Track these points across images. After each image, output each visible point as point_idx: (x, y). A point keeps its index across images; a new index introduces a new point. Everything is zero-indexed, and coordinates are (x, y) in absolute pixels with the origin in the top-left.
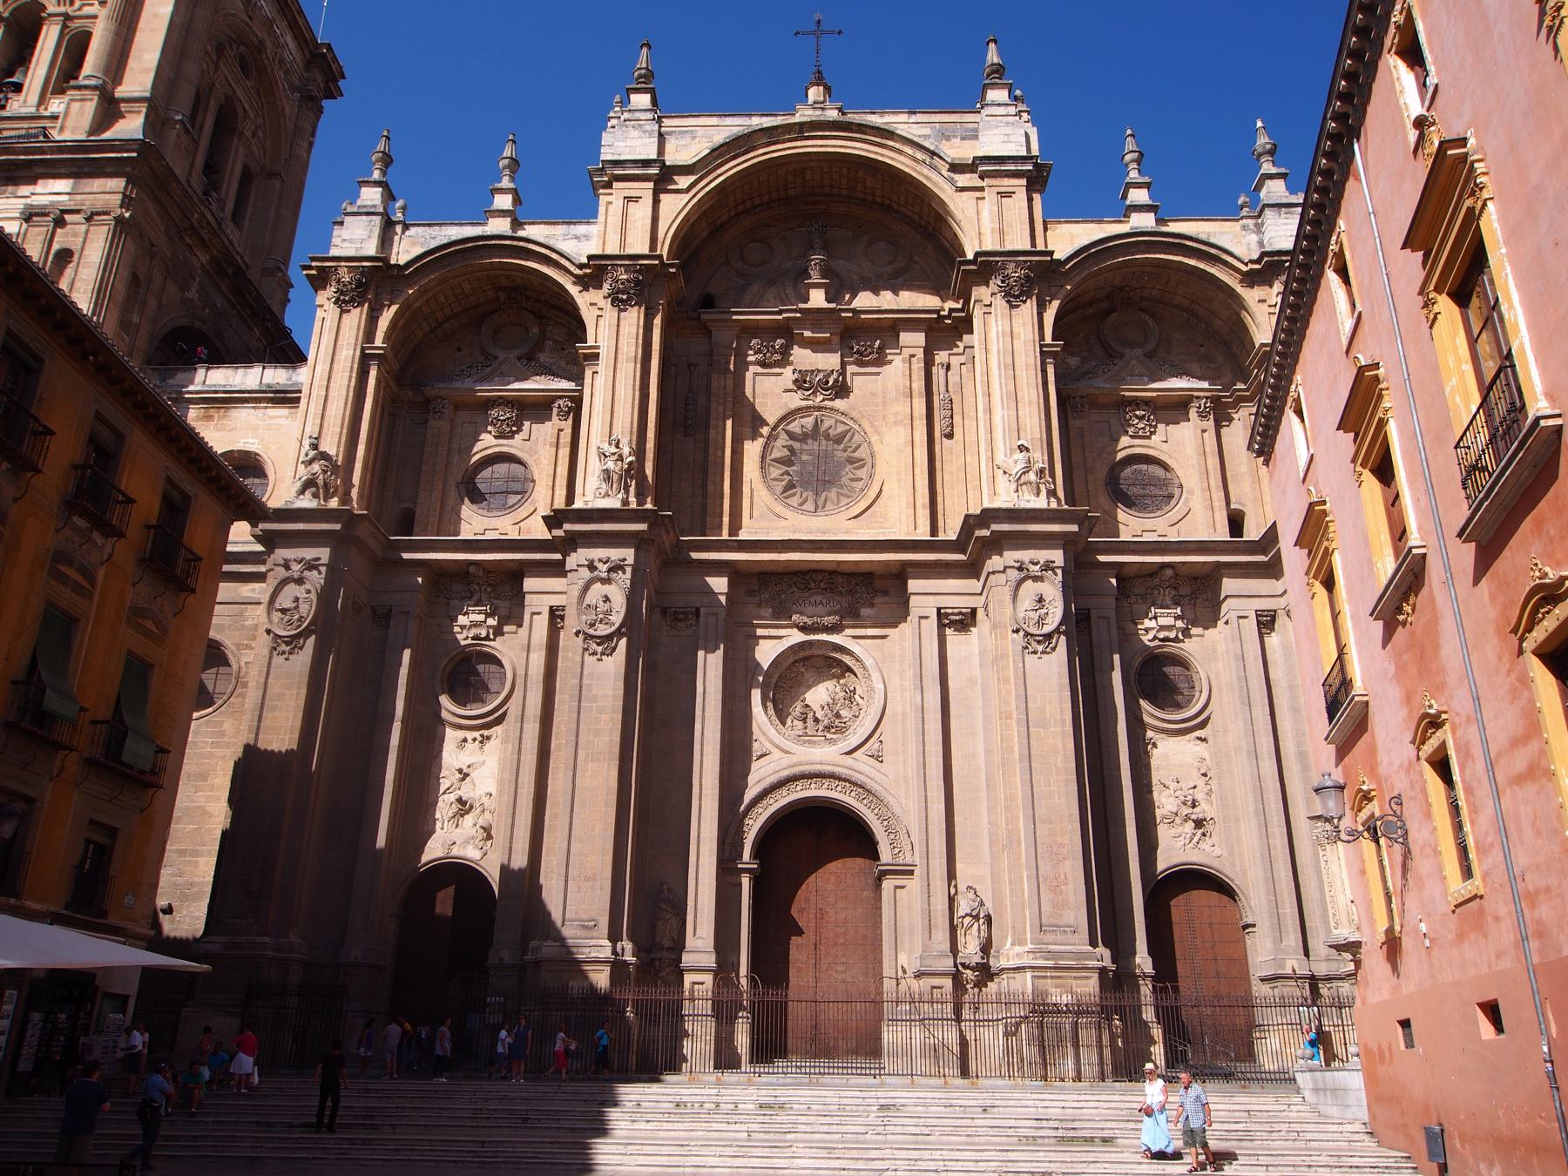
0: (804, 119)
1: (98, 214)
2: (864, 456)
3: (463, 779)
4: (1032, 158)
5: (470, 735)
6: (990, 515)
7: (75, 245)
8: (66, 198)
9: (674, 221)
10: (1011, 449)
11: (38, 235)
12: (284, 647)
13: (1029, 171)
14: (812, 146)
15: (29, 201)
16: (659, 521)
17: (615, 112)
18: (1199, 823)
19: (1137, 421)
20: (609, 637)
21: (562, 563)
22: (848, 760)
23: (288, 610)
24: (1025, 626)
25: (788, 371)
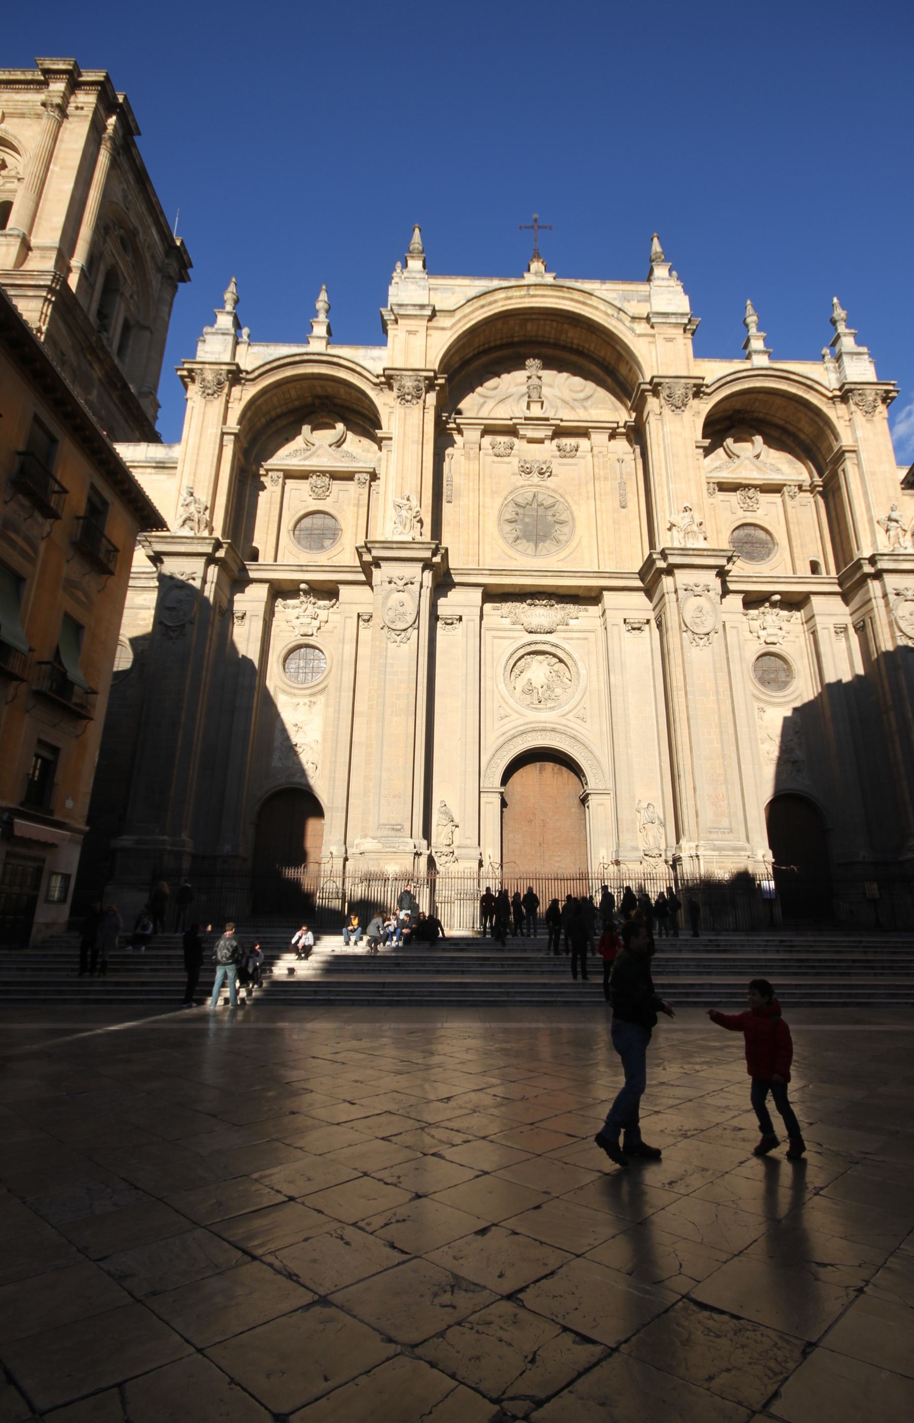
2: (567, 520)
4: (687, 314)
9: (441, 350)
10: (678, 511)
13: (686, 325)
14: (536, 302)
19: (748, 500)
21: (369, 583)
24: (691, 628)
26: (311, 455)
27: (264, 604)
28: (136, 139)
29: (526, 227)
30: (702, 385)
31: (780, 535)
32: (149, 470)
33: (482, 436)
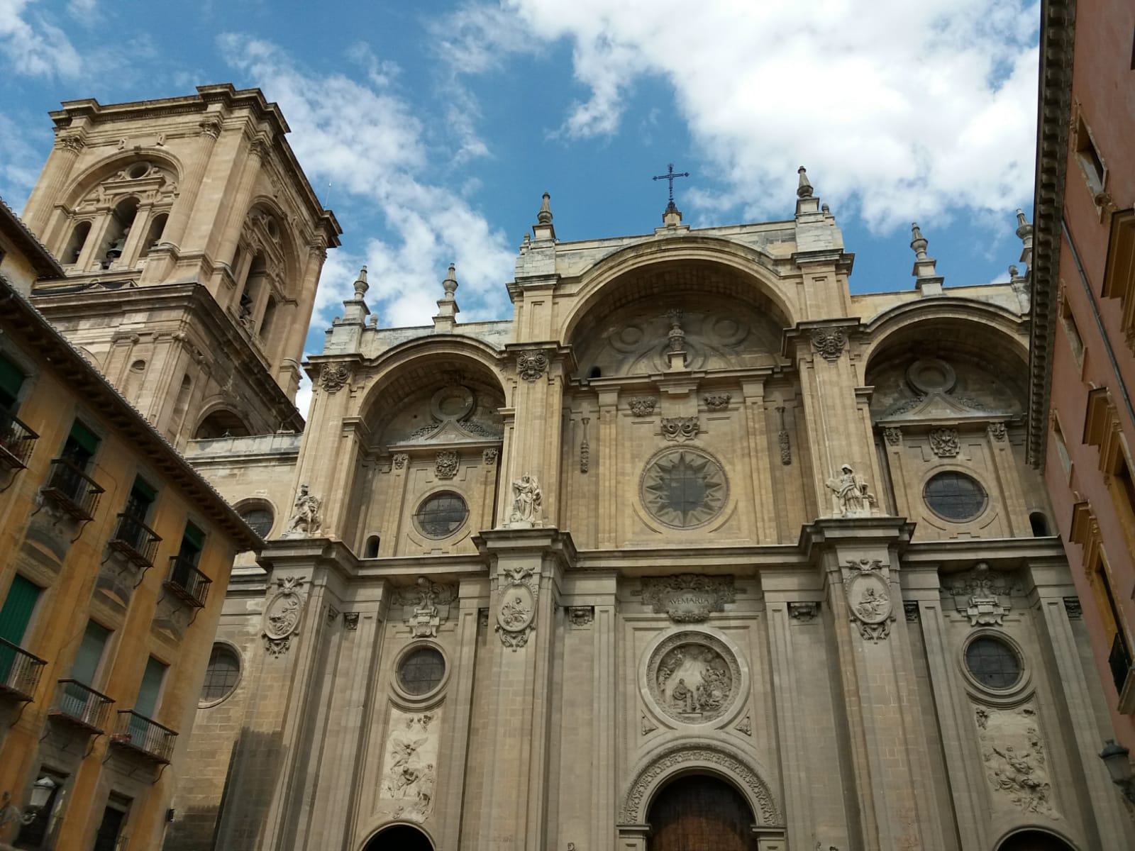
0: (662, 238)
1: (163, 335)
2: (719, 482)
3: (409, 754)
5: (416, 716)
6: (823, 525)
7: (145, 356)
8: (143, 325)
9: (567, 317)
11: (123, 351)
12: (276, 649)
14: (668, 256)
15: (117, 329)
16: (560, 537)
17: (525, 244)
18: (1033, 788)
19: (943, 445)
20: (522, 632)
22: (722, 735)
23: (279, 618)
24: (860, 617)
25: (656, 419)
26: (438, 433)
27: (378, 603)
28: (287, 135)
29: (660, 178)
30: (860, 325)
31: (989, 484)
32: (273, 464)
33: (619, 396)
